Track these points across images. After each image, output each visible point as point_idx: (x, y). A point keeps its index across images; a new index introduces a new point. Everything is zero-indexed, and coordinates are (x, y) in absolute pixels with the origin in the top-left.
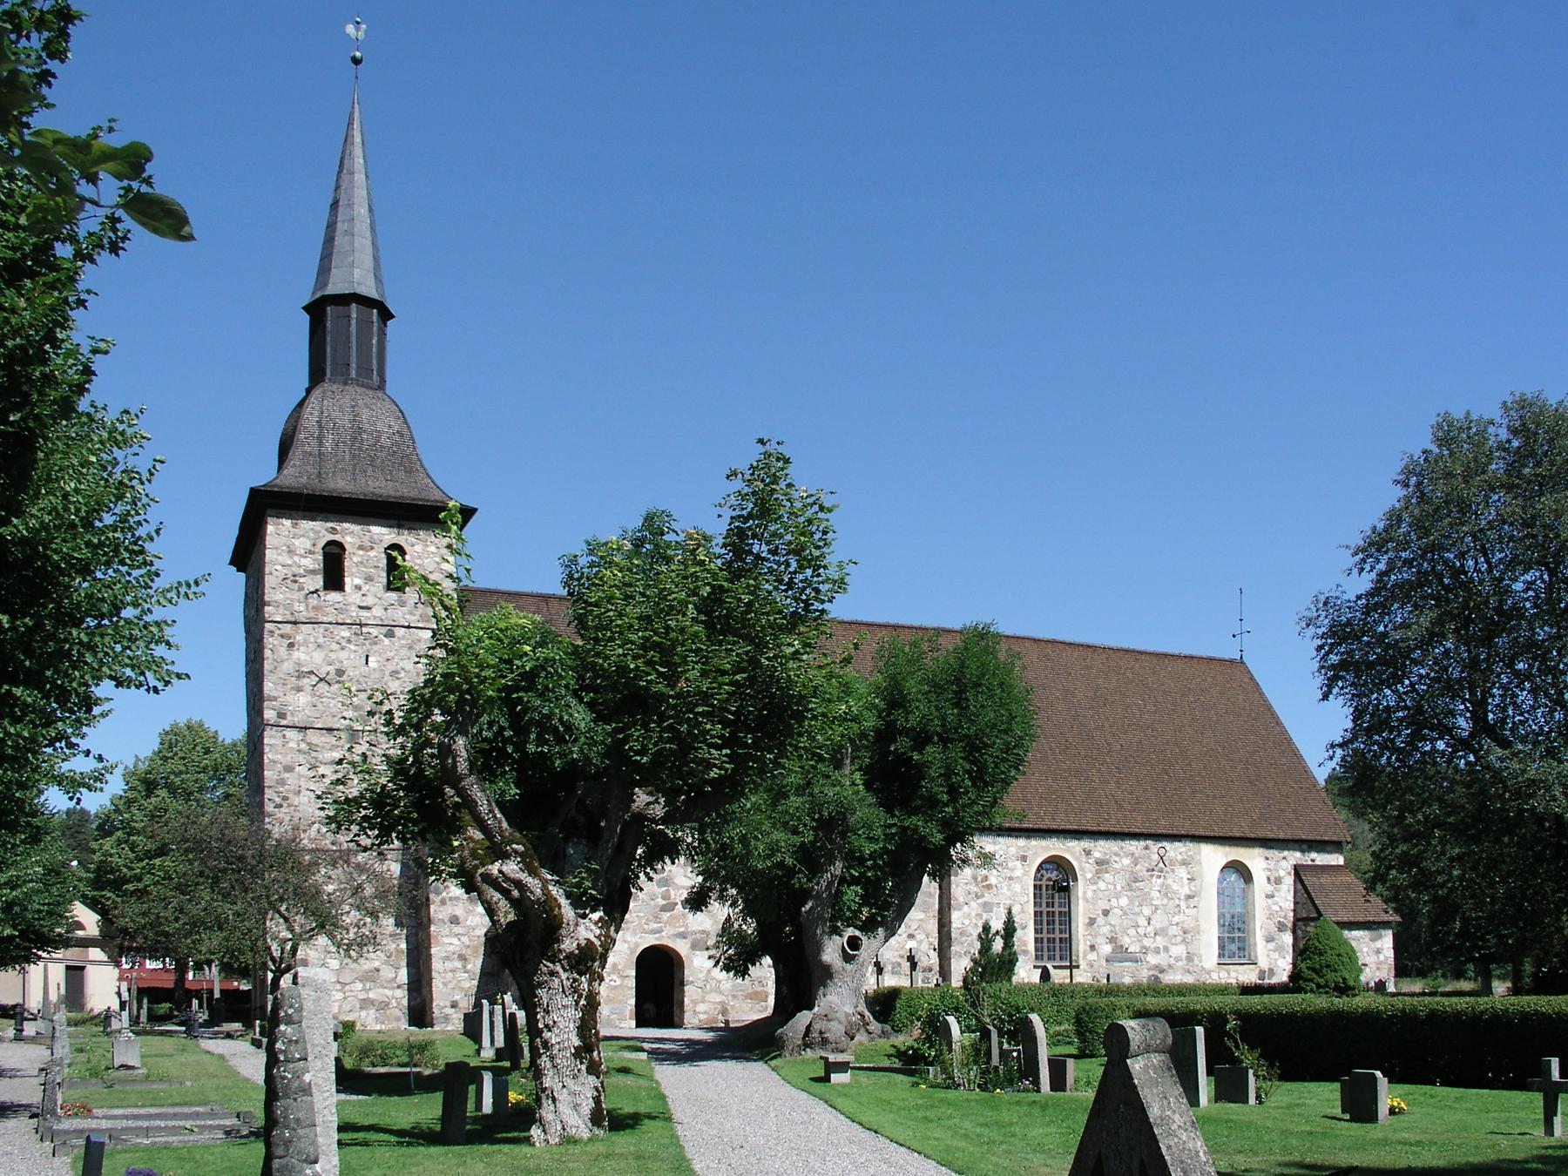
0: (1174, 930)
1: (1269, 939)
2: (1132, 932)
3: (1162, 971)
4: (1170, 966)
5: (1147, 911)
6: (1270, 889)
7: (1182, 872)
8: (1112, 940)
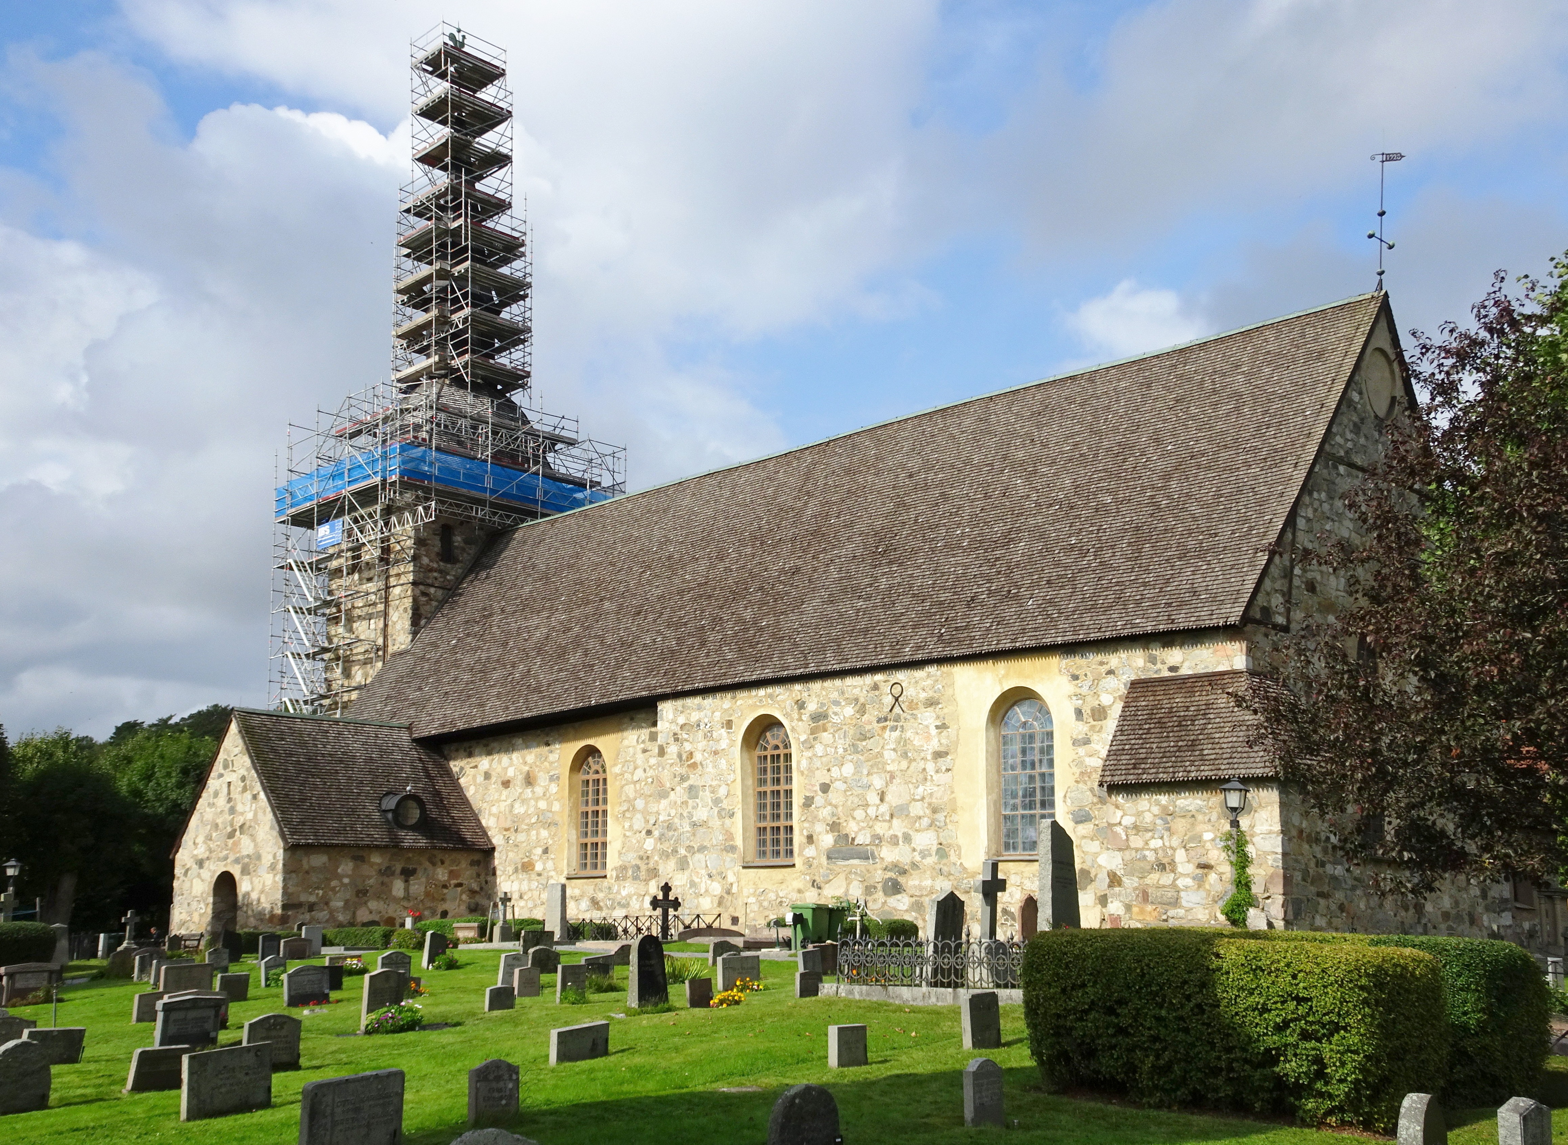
0: (917, 809)
2: (859, 814)
3: (904, 872)
4: (914, 865)
5: (878, 782)
6: (1081, 729)
7: (928, 717)
8: (834, 827)
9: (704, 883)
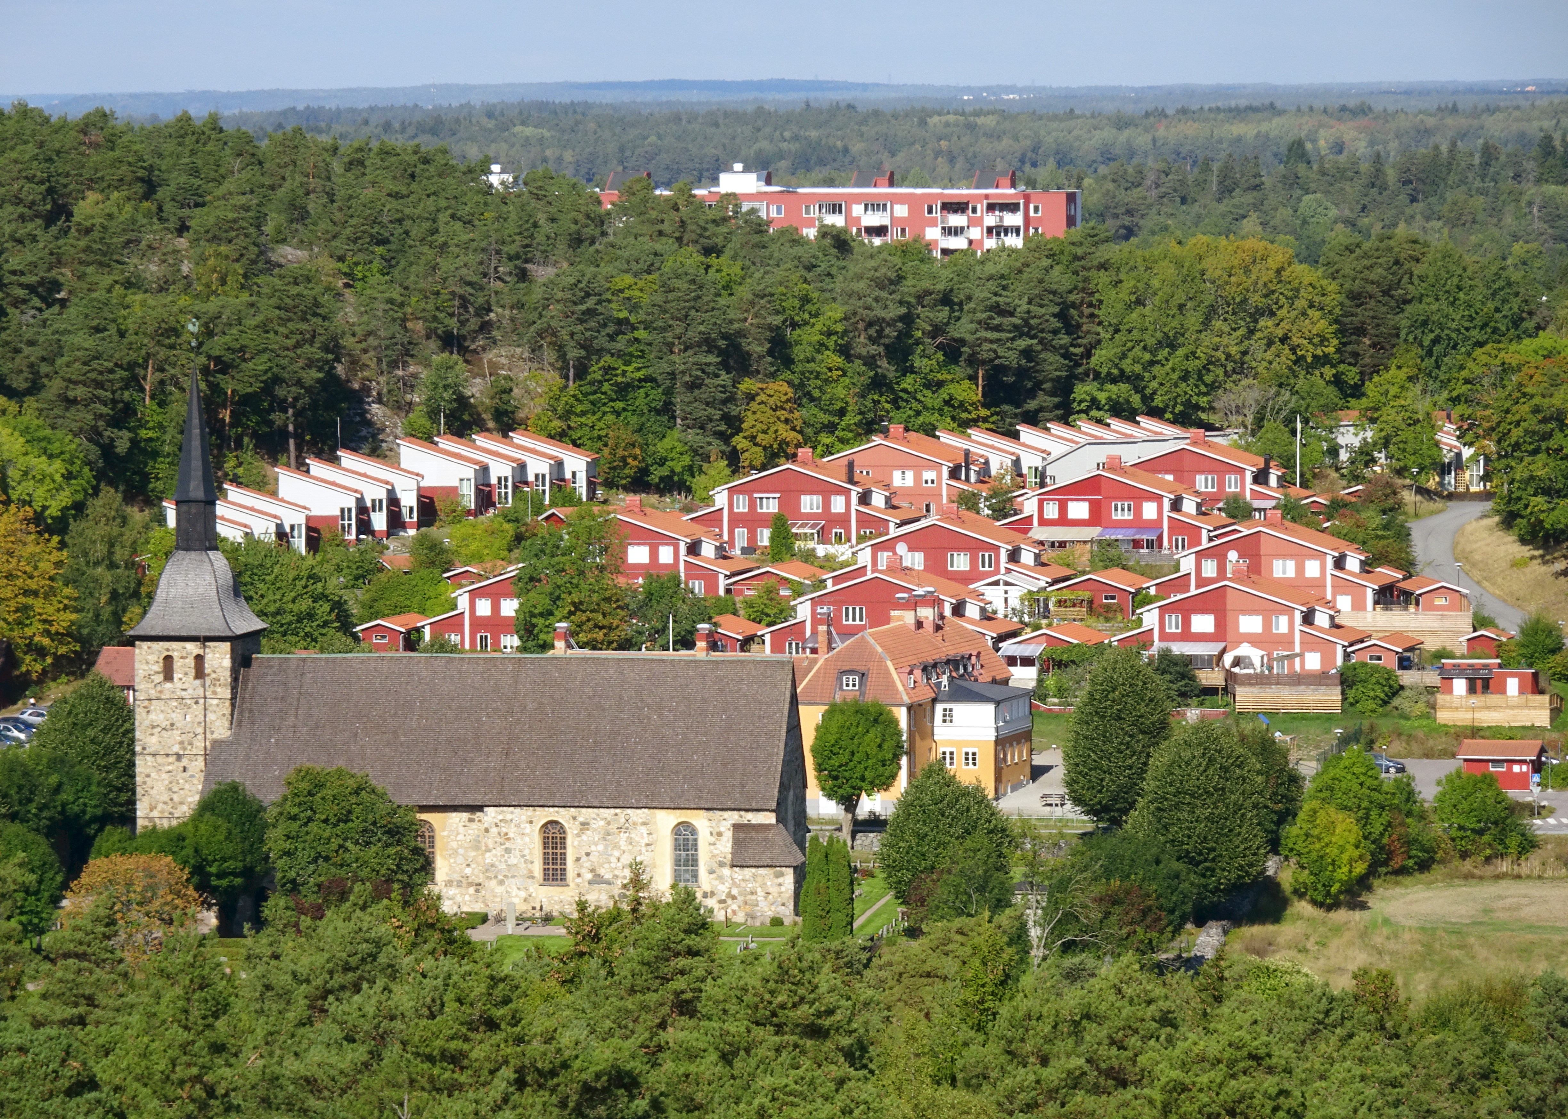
1: (711, 872)
5: (616, 853)
6: (713, 839)
7: (644, 830)
8: (592, 871)
9: (515, 892)
